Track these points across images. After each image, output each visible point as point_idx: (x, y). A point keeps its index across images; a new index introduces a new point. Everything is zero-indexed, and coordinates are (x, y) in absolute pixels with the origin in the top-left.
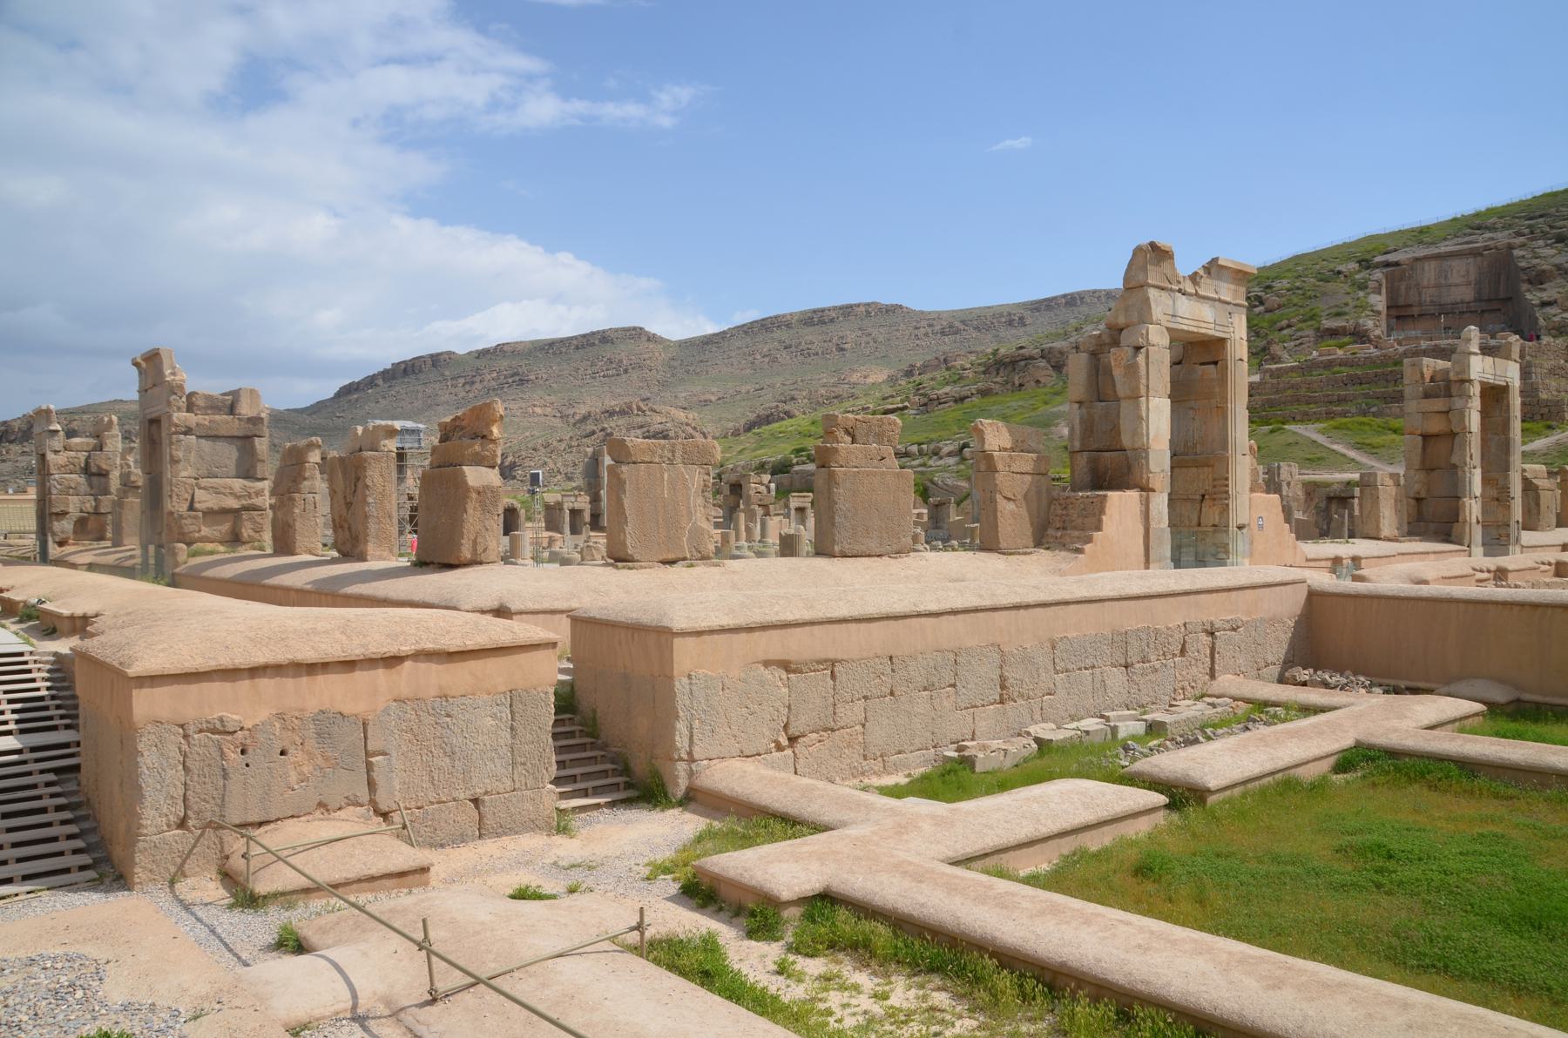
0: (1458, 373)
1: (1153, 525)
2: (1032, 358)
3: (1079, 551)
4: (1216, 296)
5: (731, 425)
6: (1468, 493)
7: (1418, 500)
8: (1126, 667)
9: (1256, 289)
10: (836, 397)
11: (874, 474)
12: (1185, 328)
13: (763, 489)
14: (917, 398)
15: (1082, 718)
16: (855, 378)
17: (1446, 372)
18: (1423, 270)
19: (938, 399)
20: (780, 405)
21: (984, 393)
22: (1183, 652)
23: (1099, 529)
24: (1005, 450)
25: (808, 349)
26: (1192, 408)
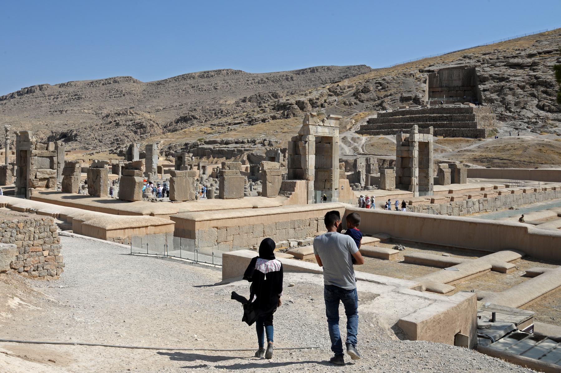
0: (411, 139)
1: (309, 189)
2: (291, 104)
3: (288, 197)
4: (330, 125)
5: (169, 120)
6: (413, 176)
7: (400, 177)
8: (294, 229)
9: (379, 79)
10: (213, 110)
11: (235, 178)
12: (320, 135)
13: (190, 159)
14: (247, 119)
15: (283, 241)
16: (221, 102)
17: (408, 138)
18: (443, 74)
19: (255, 120)
20: (190, 112)
21: (274, 118)
22: (309, 225)
23: (294, 191)
24: (269, 169)
25: (202, 88)
26: (323, 155)
